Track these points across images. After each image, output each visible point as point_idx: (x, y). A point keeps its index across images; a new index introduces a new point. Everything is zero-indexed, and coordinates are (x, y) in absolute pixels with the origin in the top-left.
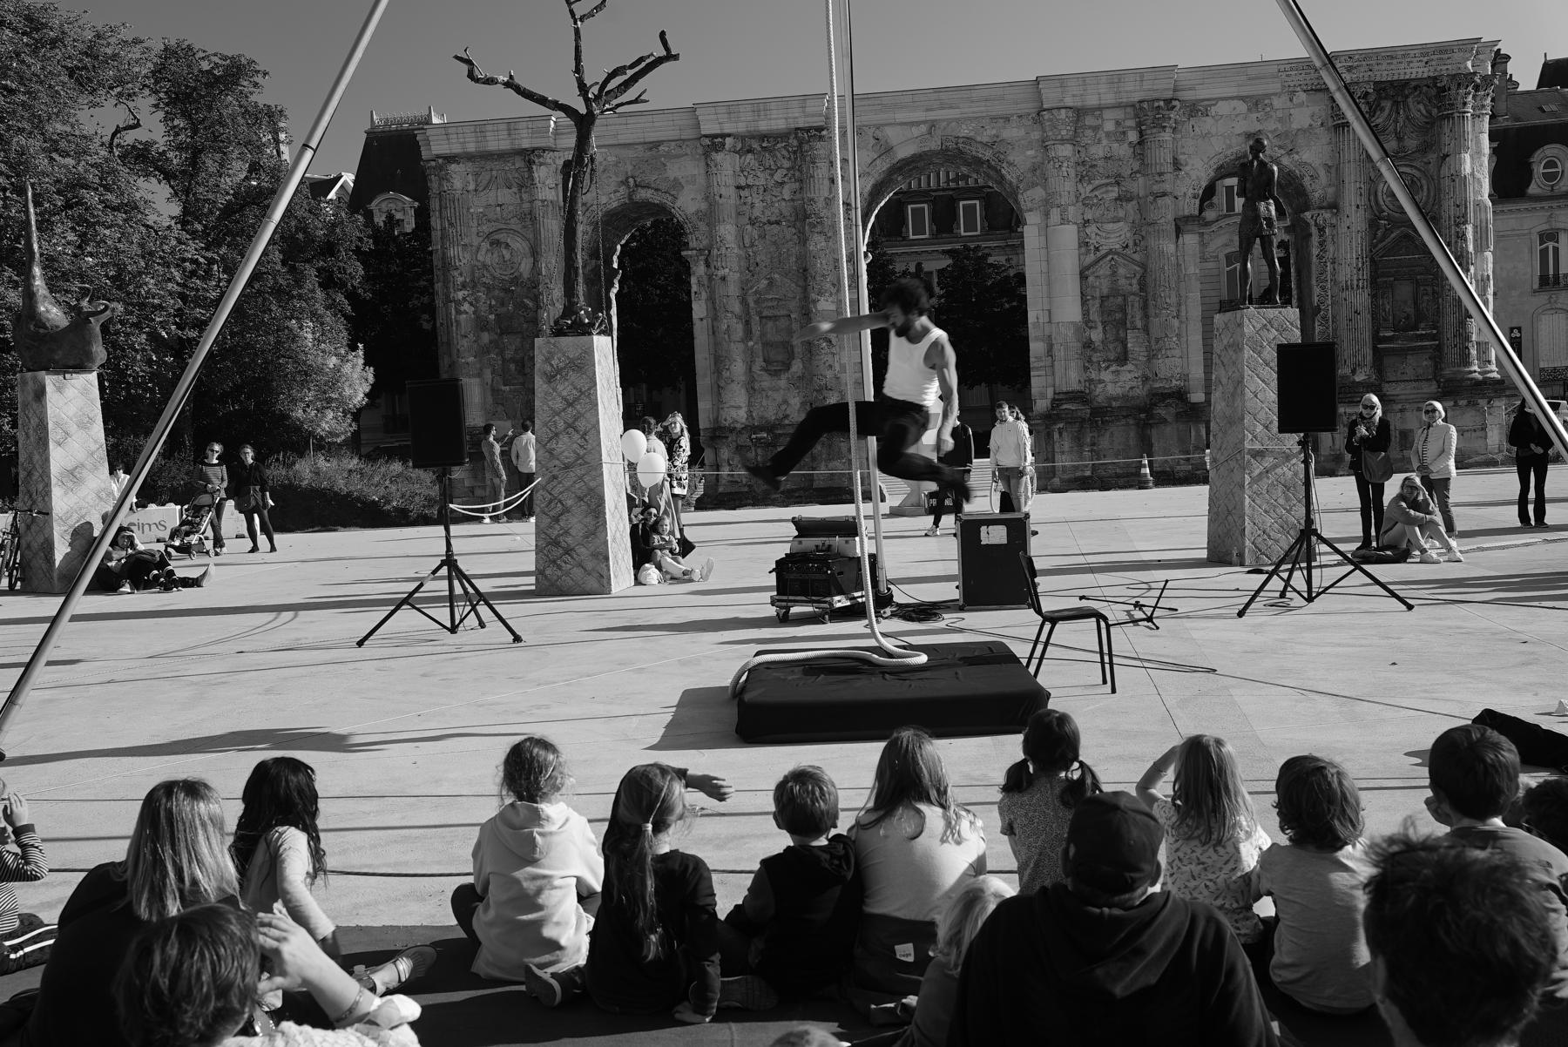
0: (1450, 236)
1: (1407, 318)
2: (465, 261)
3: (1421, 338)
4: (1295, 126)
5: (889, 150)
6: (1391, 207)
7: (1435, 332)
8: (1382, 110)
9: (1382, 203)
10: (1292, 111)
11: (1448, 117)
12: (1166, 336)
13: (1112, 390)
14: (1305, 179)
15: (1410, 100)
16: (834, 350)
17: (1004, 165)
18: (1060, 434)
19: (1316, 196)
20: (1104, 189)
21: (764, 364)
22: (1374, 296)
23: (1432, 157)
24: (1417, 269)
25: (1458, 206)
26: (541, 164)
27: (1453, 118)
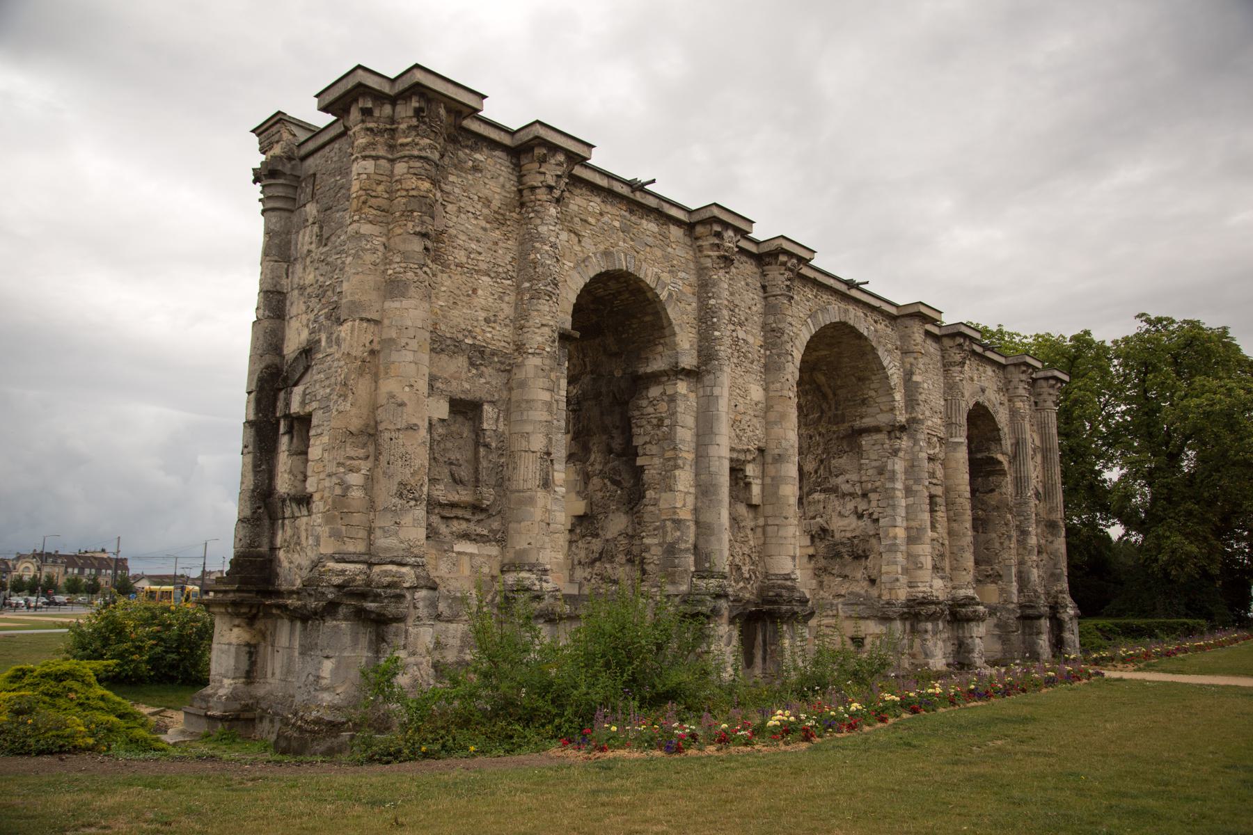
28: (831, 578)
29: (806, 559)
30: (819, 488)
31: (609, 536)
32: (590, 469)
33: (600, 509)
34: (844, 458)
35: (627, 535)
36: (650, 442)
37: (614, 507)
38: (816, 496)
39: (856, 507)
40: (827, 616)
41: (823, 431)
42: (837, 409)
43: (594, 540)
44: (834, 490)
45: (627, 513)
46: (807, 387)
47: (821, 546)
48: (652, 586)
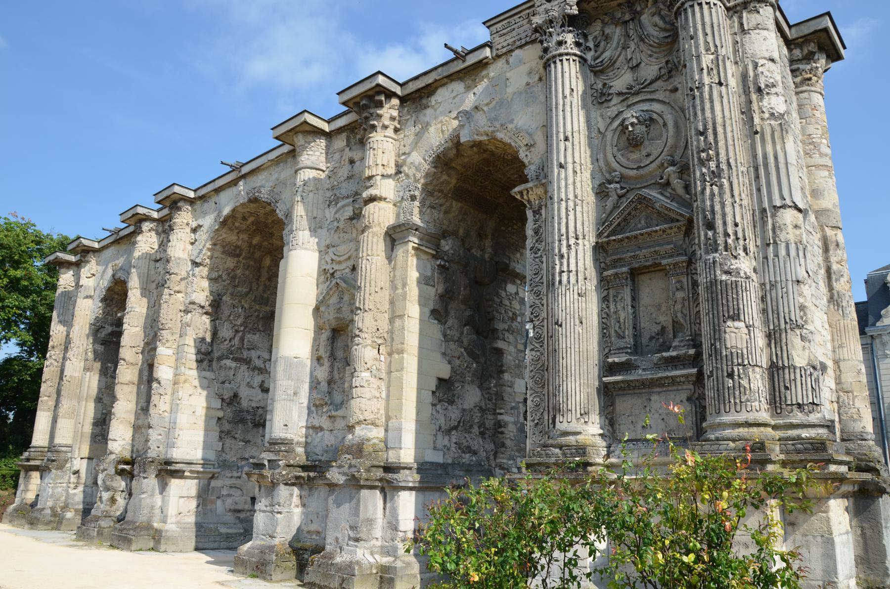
0: (695, 183)
1: (663, 329)
2: (57, 332)
3: (673, 362)
4: (510, 90)
5: (220, 212)
6: (623, 161)
7: (692, 352)
8: (607, 38)
9: (611, 159)
10: (508, 75)
11: (677, 14)
12: (355, 371)
13: (328, 439)
14: (521, 151)
15: (645, 18)
16: (161, 391)
17: (278, 205)
18: (260, 487)
19: (530, 171)
20: (342, 211)
21: (145, 404)
22: (604, 300)
23: (676, 81)
24: (662, 250)
25: (702, 134)
26: (88, 262)
27: (686, 10)
28: (233, 441)
29: (215, 421)
30: (232, 356)
31: (466, 406)
32: (448, 332)
33: (458, 377)
34: (258, 335)
35: (481, 408)
36: (508, 331)
37: (470, 379)
38: (228, 362)
39: (263, 381)
40: (232, 477)
41: (246, 306)
42: (264, 292)
43: (450, 407)
44: (247, 362)
45: (479, 387)
46: (252, 263)
47: (229, 412)
48: (509, 459)
